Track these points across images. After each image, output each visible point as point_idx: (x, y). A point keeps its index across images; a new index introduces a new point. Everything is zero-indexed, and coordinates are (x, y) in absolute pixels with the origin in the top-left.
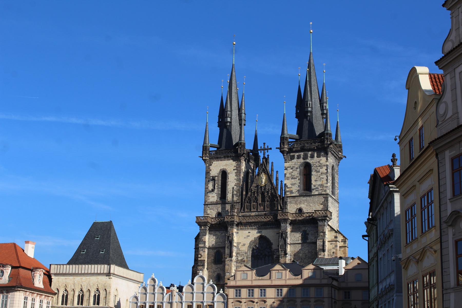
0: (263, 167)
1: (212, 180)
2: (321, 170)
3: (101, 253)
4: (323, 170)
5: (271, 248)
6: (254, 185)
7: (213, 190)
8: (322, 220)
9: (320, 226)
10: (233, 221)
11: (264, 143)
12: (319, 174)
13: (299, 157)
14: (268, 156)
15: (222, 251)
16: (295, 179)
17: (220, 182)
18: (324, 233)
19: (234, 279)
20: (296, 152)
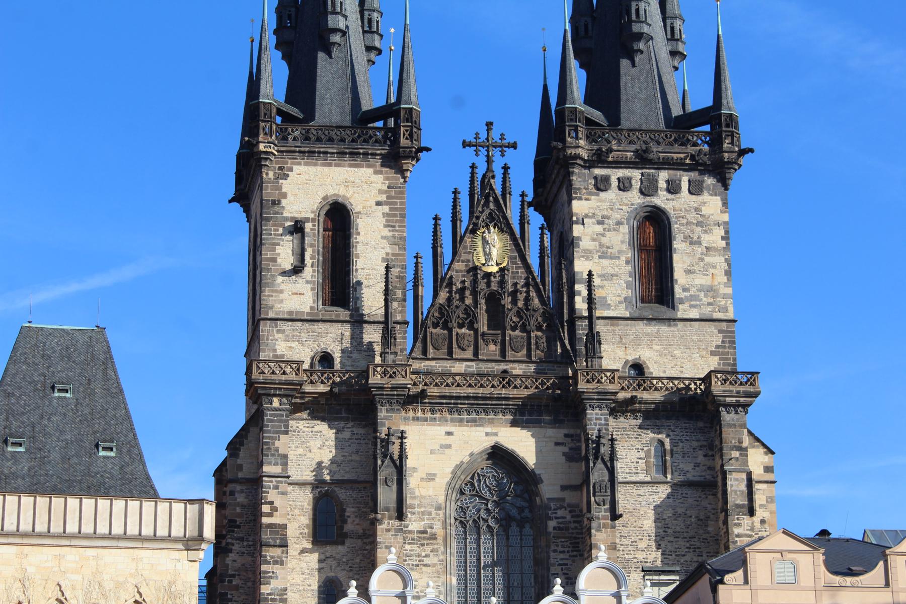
0: (492, 206)
1: (291, 233)
2: (706, 239)
3: (102, 453)
4: (715, 237)
5: (538, 494)
6: (459, 266)
7: (297, 270)
8: (736, 406)
9: (730, 426)
10: (404, 387)
11: (489, 125)
12: (699, 250)
13: (624, 185)
14: (506, 168)
15: (342, 494)
16: (611, 258)
17: (321, 240)
18: (743, 450)
19: (746, 582)
20: (618, 164)
